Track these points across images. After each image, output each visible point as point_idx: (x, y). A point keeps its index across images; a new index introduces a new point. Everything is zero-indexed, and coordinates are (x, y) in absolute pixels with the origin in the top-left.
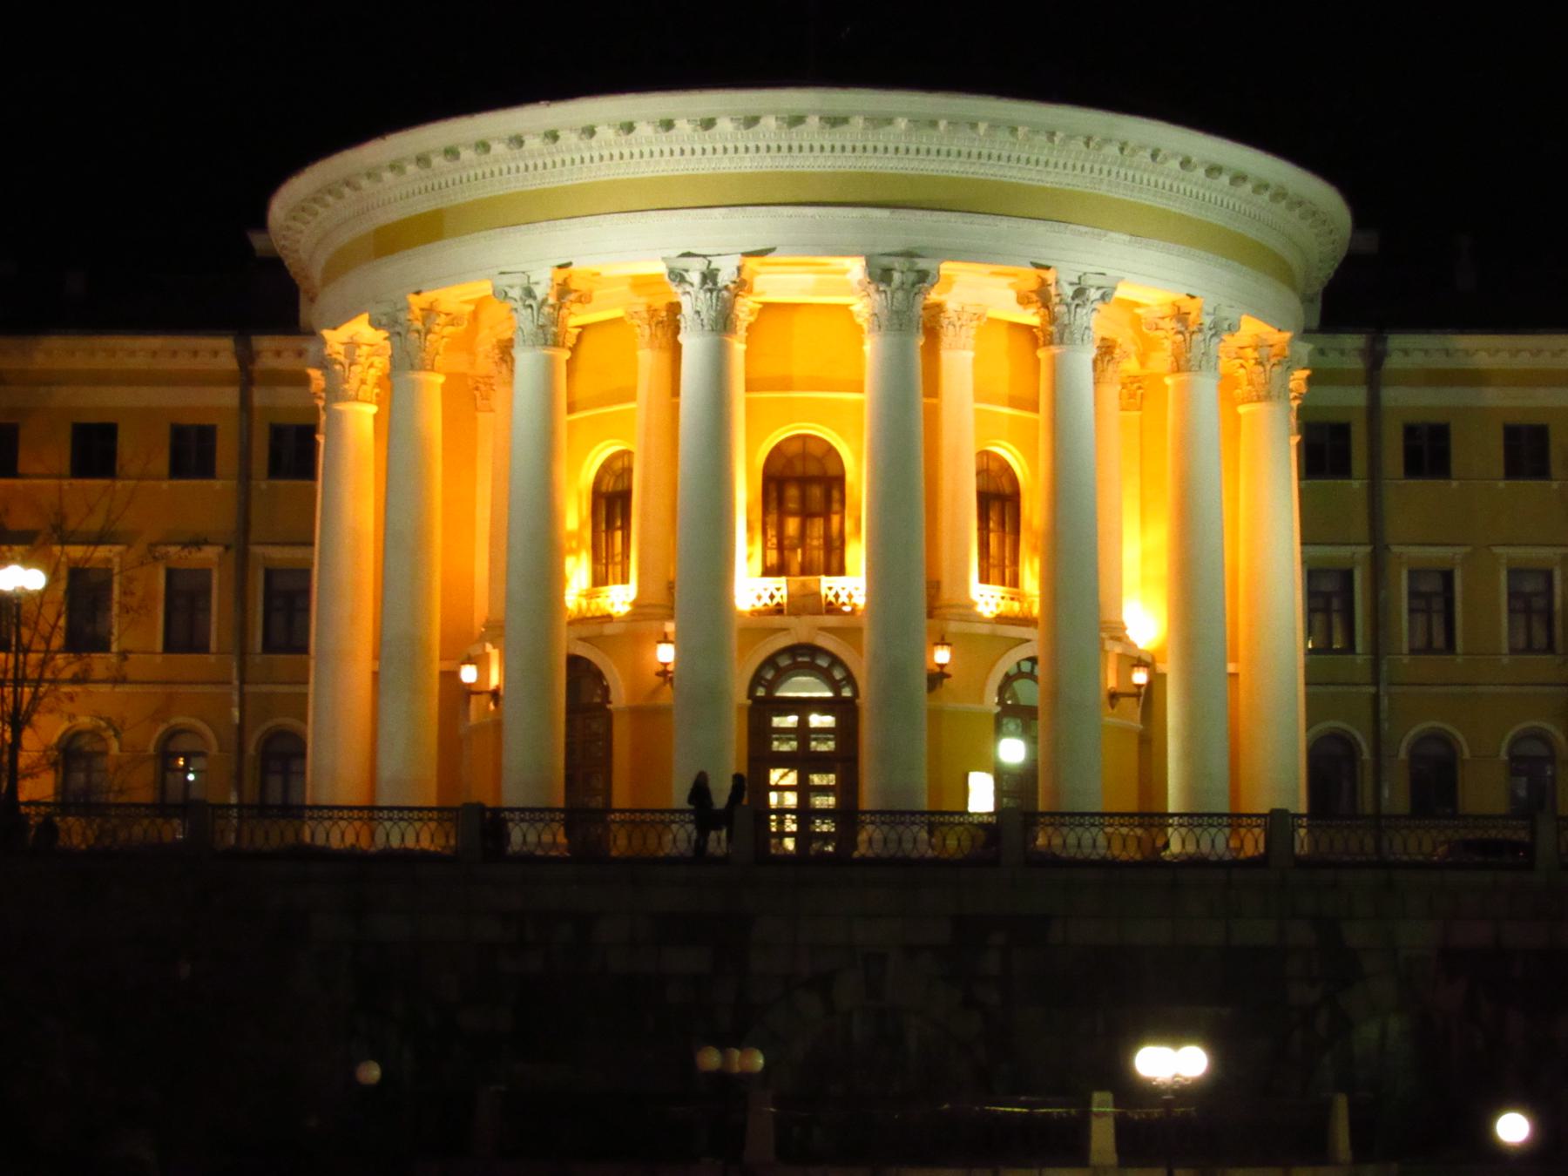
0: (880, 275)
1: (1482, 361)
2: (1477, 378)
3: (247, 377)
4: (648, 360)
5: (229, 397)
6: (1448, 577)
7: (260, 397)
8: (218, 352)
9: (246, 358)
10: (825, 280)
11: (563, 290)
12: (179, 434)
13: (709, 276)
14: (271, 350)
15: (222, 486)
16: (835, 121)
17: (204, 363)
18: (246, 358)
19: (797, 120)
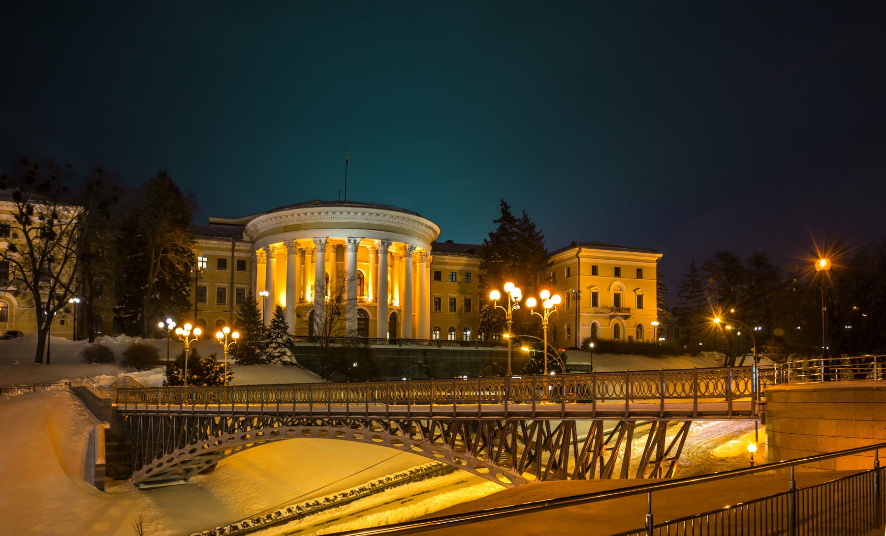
0: (383, 243)
1: (447, 261)
2: (446, 264)
3: (233, 250)
4: (372, 256)
5: (230, 254)
6: (440, 299)
7: (236, 254)
8: (229, 245)
9: (234, 246)
10: (371, 243)
11: (326, 242)
12: (219, 260)
13: (355, 241)
14: (239, 246)
15: (228, 272)
16: (378, 215)
17: (224, 247)
18: (234, 246)
19: (371, 214)
